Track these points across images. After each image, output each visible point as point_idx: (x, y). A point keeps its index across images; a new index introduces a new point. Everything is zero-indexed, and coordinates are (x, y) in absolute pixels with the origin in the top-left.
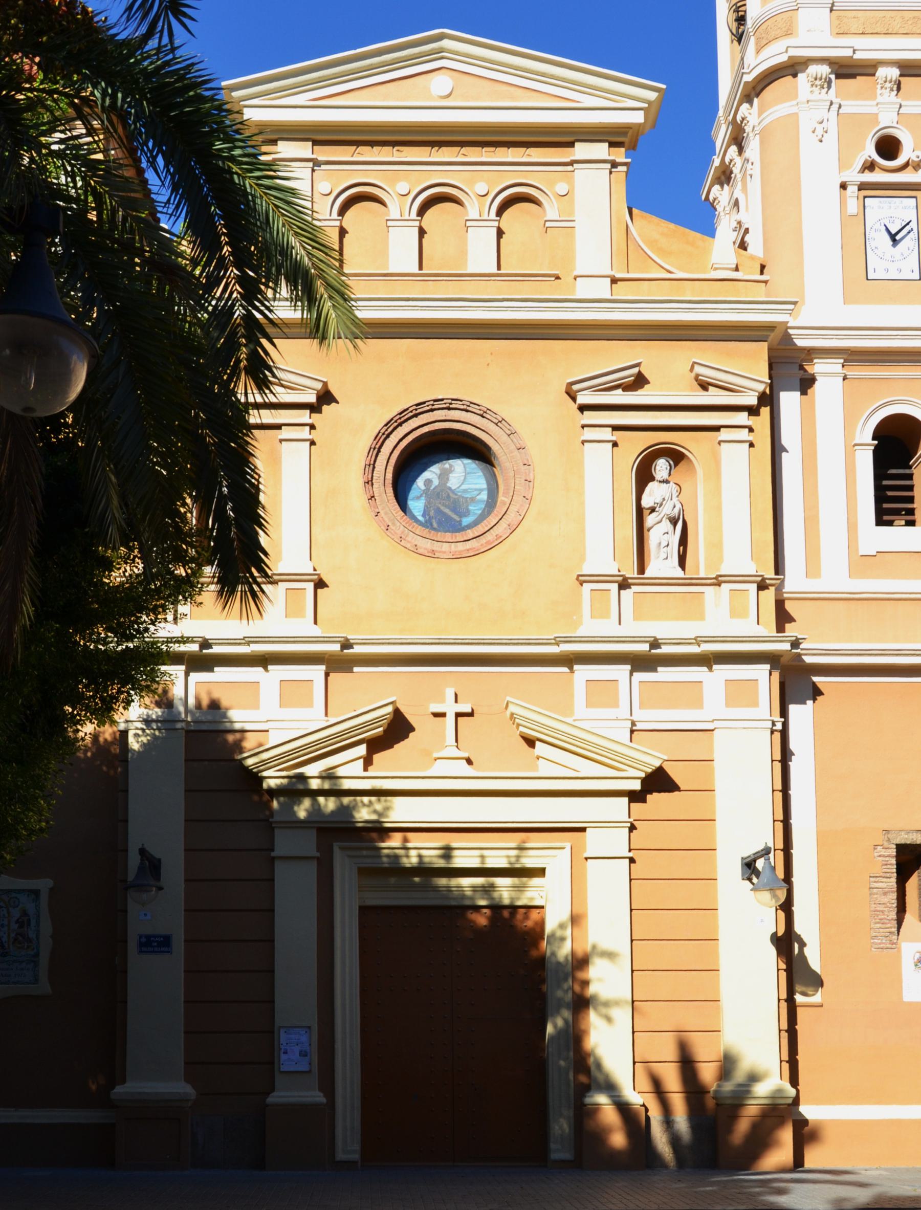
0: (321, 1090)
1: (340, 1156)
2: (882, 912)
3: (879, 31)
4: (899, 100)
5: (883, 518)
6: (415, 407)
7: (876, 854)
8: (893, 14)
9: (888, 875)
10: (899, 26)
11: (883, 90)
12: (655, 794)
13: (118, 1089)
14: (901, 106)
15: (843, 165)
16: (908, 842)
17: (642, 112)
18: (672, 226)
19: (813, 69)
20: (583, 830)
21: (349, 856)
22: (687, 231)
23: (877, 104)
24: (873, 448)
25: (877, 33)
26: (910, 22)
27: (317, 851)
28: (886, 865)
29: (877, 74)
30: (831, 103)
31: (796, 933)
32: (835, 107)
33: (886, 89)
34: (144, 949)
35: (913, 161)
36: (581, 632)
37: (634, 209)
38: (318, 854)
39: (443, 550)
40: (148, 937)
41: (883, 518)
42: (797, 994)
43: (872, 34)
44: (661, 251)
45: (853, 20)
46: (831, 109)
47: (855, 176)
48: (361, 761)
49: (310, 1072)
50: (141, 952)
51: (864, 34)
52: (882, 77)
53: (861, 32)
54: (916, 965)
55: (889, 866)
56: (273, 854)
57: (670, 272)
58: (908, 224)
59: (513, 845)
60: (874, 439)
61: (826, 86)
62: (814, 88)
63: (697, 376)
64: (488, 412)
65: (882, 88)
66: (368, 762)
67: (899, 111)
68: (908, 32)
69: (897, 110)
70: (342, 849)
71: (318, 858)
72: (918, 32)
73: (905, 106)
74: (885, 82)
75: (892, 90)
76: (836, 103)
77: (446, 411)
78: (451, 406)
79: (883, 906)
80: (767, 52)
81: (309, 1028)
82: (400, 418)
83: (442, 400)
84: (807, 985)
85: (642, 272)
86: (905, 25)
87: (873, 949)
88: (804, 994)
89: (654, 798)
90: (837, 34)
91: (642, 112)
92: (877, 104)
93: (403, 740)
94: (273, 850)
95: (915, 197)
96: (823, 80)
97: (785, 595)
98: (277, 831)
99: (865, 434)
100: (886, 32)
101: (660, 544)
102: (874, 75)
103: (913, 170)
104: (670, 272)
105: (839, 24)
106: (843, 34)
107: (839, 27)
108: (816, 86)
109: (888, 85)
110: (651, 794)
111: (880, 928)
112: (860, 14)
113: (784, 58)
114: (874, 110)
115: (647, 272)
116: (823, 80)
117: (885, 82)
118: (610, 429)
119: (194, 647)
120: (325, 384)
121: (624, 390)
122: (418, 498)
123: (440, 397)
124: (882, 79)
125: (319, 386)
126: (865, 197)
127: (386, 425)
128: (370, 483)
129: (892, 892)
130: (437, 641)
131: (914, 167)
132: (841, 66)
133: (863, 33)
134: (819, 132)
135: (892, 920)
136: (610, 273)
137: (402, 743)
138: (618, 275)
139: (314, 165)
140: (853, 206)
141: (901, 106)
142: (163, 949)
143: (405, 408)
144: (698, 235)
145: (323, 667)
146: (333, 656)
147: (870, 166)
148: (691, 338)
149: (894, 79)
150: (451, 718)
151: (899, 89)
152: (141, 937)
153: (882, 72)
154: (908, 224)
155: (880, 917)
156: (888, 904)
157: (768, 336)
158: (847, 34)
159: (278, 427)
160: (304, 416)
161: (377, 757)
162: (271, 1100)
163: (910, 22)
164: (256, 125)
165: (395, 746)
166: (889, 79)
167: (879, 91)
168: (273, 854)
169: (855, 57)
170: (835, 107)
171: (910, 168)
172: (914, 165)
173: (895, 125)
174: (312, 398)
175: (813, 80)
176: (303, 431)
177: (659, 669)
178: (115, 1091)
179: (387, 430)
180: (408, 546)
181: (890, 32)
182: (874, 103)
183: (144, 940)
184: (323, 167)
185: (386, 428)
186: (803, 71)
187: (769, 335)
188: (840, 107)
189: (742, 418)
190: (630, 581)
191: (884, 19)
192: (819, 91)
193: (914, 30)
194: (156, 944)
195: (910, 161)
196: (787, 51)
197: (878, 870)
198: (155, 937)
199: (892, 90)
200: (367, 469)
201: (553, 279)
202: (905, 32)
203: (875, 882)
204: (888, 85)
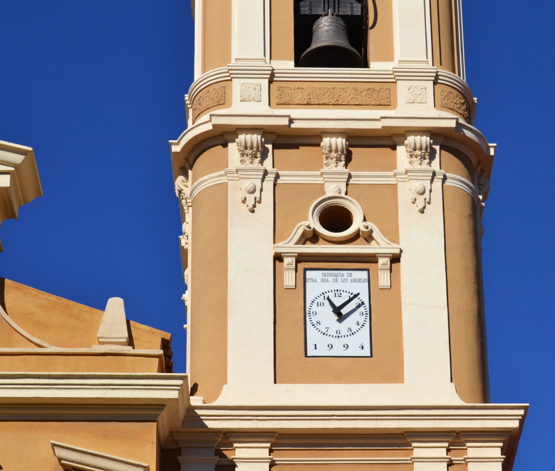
3: (327, 102)
4: (347, 171)
10: (350, 97)
11: (329, 161)
14: (350, 177)
18: (53, 298)
19: (242, 138)
22: (72, 303)
23: (322, 174)
25: (324, 104)
26: (364, 94)
29: (322, 144)
30: (266, 173)
32: (270, 178)
33: (332, 159)
35: (362, 231)
37: (6, 280)
43: (319, 104)
45: (296, 90)
46: (266, 179)
51: (310, 105)
52: (325, 146)
53: (305, 103)
57: (40, 346)
58: (356, 296)
61: (259, 155)
62: (245, 157)
63: (60, 459)
65: (327, 158)
67: (348, 181)
68: (361, 103)
69: (346, 180)
72: (373, 103)
73: (356, 176)
74: (330, 151)
75: (339, 160)
76: (272, 173)
85: (5, 346)
86: (358, 97)
90: (277, 104)
92: (322, 174)
95: (368, 270)
96: (255, 149)
100: (335, 103)
102: (319, 145)
103: (365, 241)
104: (40, 346)
105: (281, 95)
106: (284, 104)
107: (280, 97)
108: (247, 156)
109: (333, 155)
112: (305, 85)
113: (209, 127)
114: (320, 180)
115: (11, 347)
116: (255, 149)
117: (330, 151)
124: (325, 149)
131: (365, 239)
132: (280, 136)
133: (307, 104)
134: (250, 202)
141: (350, 177)
144: (86, 308)
148: (58, 419)
149: (340, 148)
151: (348, 159)
153: (326, 141)
154: (356, 296)
157: (157, 416)
158: (289, 104)
163: (364, 94)
166: (334, 148)
167: (325, 162)
169: (293, 126)
170: (270, 178)
171: (361, 239)
172: (366, 236)
173: (343, 195)
175: (243, 149)
181: (339, 103)
182: (319, 173)
186: (233, 141)
187: (159, 415)
188: (277, 177)
191: (333, 90)
192: (251, 161)
193: (369, 101)
195: (360, 232)
196: (210, 121)
199: (339, 160)
202: (358, 103)
204: (333, 155)
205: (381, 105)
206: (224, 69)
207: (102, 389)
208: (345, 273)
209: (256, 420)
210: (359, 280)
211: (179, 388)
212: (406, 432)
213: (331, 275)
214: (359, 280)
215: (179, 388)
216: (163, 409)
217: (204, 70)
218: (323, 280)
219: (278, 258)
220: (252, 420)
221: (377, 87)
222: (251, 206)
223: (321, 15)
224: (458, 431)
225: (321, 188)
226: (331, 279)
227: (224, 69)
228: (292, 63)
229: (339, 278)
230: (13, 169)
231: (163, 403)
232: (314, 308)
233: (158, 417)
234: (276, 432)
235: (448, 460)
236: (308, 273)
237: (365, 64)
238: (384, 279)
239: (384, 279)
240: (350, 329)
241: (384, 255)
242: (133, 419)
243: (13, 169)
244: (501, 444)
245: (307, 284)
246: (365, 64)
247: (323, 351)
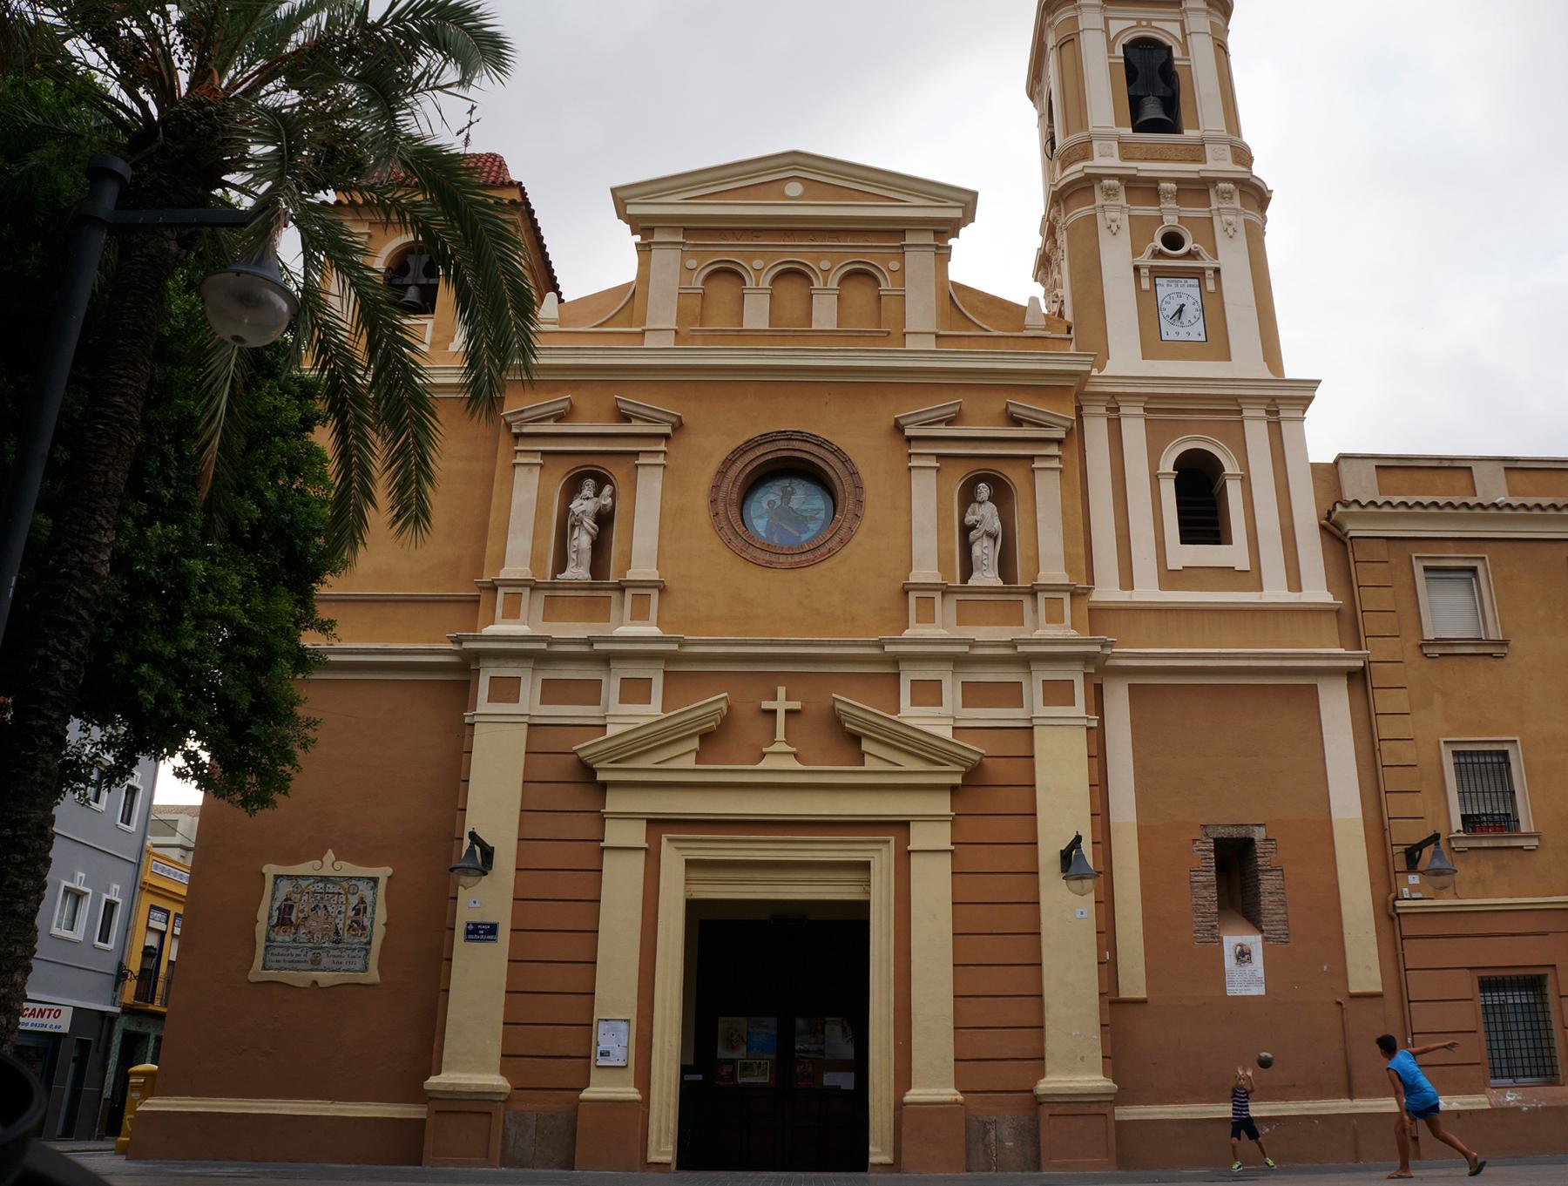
0: (635, 1087)
1: (653, 1157)
2: (1204, 905)
5: (1188, 536)
8: (1169, 146)
9: (1208, 869)
13: (433, 1080)
15: (1136, 253)
17: (961, 210)
21: (677, 848)
24: (1174, 477)
27: (646, 842)
28: (1205, 859)
34: (471, 937)
36: (907, 634)
38: (646, 845)
39: (781, 561)
40: (475, 925)
41: (1188, 536)
44: (981, 315)
47: (1145, 260)
48: (694, 755)
49: (626, 1067)
50: (467, 939)
54: (1238, 959)
55: (1208, 860)
56: (602, 844)
60: (1174, 470)
70: (670, 840)
71: (646, 849)
80: (1067, 172)
81: (628, 1021)
83: (785, 432)
91: (961, 210)
94: (603, 841)
98: (608, 822)
99: (1167, 465)
112: (1143, 146)
118: (935, 457)
121: (946, 425)
122: (761, 517)
123: (783, 430)
126: (1155, 277)
127: (732, 453)
136: (935, 330)
138: (941, 333)
140: (1146, 284)
142: (489, 937)
143: (751, 438)
147: (1158, 254)
150: (781, 717)
152: (468, 924)
155: (1204, 910)
162: (584, 1095)
167: (1162, 200)
168: (602, 844)
176: (658, 457)
178: (429, 1081)
180: (748, 557)
183: (471, 927)
189: (1054, 450)
194: (482, 932)
196: (1083, 170)
198: (482, 925)
203: (1196, 876)
205: (1194, 160)
206: (1085, 134)
208: (1183, 280)
210: (1193, 286)
213: (1173, 282)
214: (1193, 286)
217: (1067, 132)
218: (1168, 285)
219: (1137, 269)
221: (1192, 148)
222: (1114, 231)
223: (1142, 97)
225: (1160, 220)
226: (1173, 284)
227: (1085, 134)
228: (1131, 129)
229: (1179, 284)
232: (1164, 305)
236: (1157, 279)
237: (1180, 132)
238: (1211, 286)
239: (1211, 286)
240: (1190, 321)
241: (1210, 268)
245: (1158, 287)
246: (1180, 132)
247: (1173, 337)
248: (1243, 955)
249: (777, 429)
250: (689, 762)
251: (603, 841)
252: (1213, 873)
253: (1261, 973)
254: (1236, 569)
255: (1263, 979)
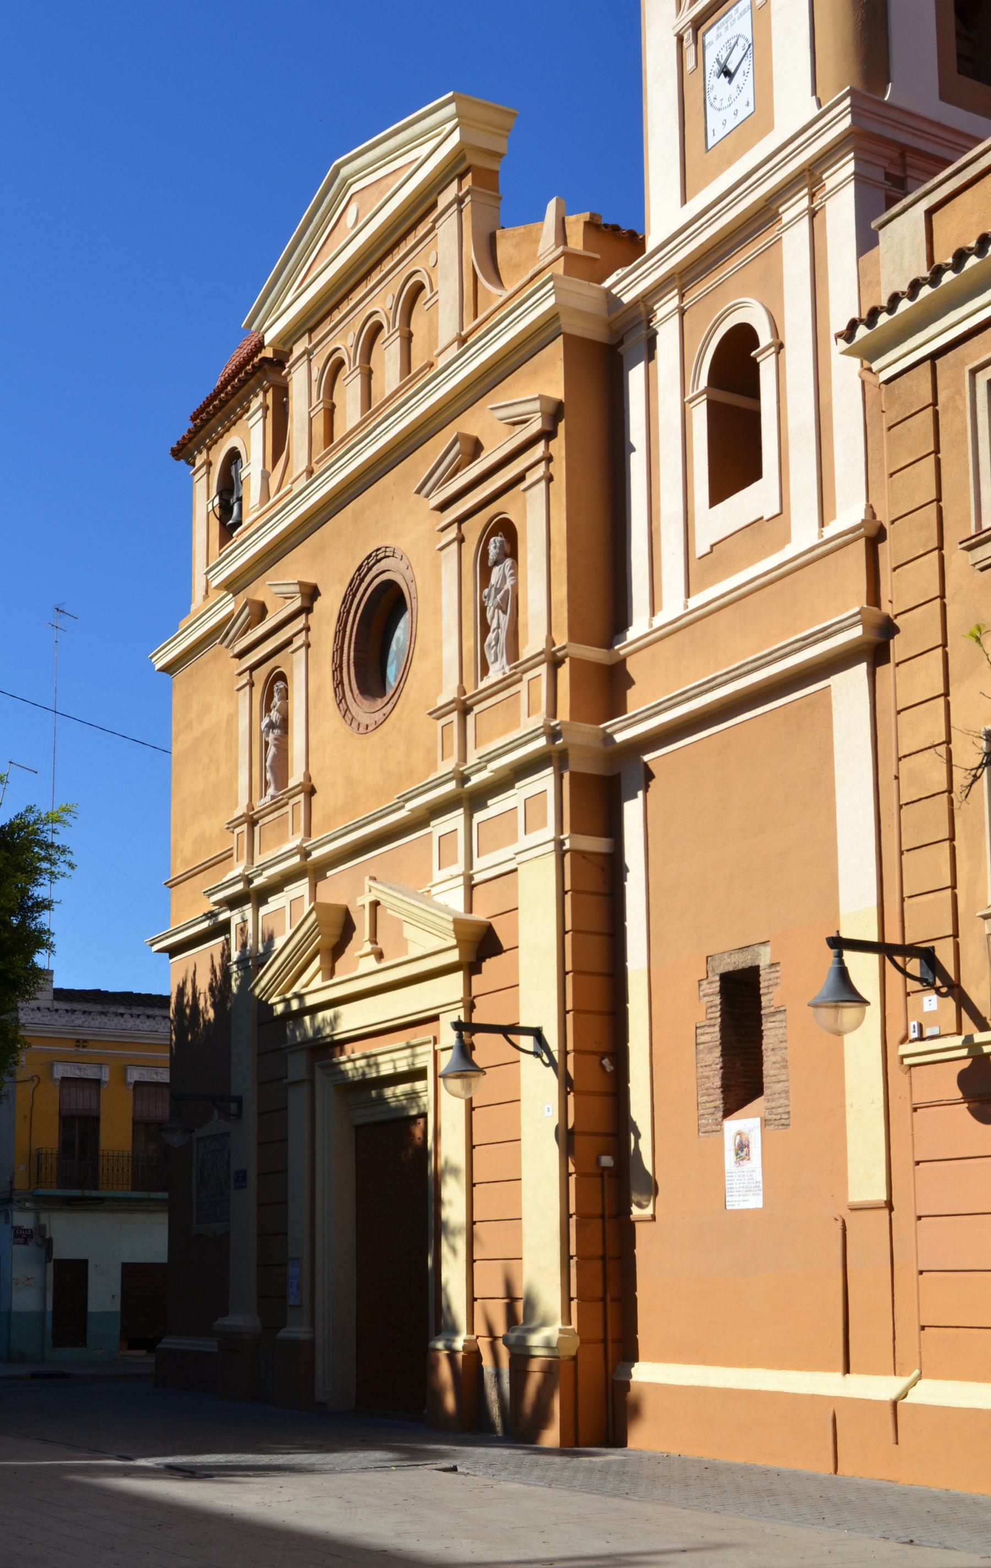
2: (708, 1077)
6: (357, 573)
7: (702, 993)
12: (488, 960)
16: (731, 969)
20: (435, 1018)
31: (632, 1120)
42: (633, 1205)
56: (285, 1081)
59: (403, 1044)
64: (378, 553)
66: (332, 973)
77: (378, 564)
78: (379, 557)
79: (708, 1069)
82: (351, 590)
84: (641, 1193)
87: (701, 1134)
88: (640, 1206)
89: (489, 965)
93: (349, 942)
94: (286, 1077)
97: (622, 652)
101: (489, 645)
110: (485, 961)
111: (707, 1102)
119: (240, 887)
120: (300, 584)
125: (297, 588)
128: (338, 669)
129: (716, 1047)
130: (345, 830)
135: (717, 1088)
137: (350, 945)
139: (309, 356)
145: (307, 880)
146: (317, 863)
148: (513, 369)
155: (707, 1085)
156: (713, 1066)
159: (288, 642)
160: (299, 623)
161: (338, 964)
164: (279, 342)
165: (346, 950)
174: (297, 603)
177: (490, 802)
179: (345, 607)
184: (315, 352)
185: (344, 606)
187: (560, 325)
190: (469, 702)
197: (701, 1018)
200: (335, 656)
201: (428, 369)
207: (510, 329)
209: (654, 270)
211: (552, 291)
212: (767, 200)
215: (552, 291)
216: (559, 318)
220: (650, 273)
224: (806, 166)
230: (457, 120)
231: (555, 312)
233: (561, 328)
234: (674, 274)
235: (807, 212)
242: (548, 341)
243: (457, 120)
244: (852, 155)
248: (742, 1148)
249: (375, 548)
250: (318, 982)
251: (286, 1077)
252: (717, 1028)
253: (758, 1176)
254: (765, 518)
255: (761, 1185)
